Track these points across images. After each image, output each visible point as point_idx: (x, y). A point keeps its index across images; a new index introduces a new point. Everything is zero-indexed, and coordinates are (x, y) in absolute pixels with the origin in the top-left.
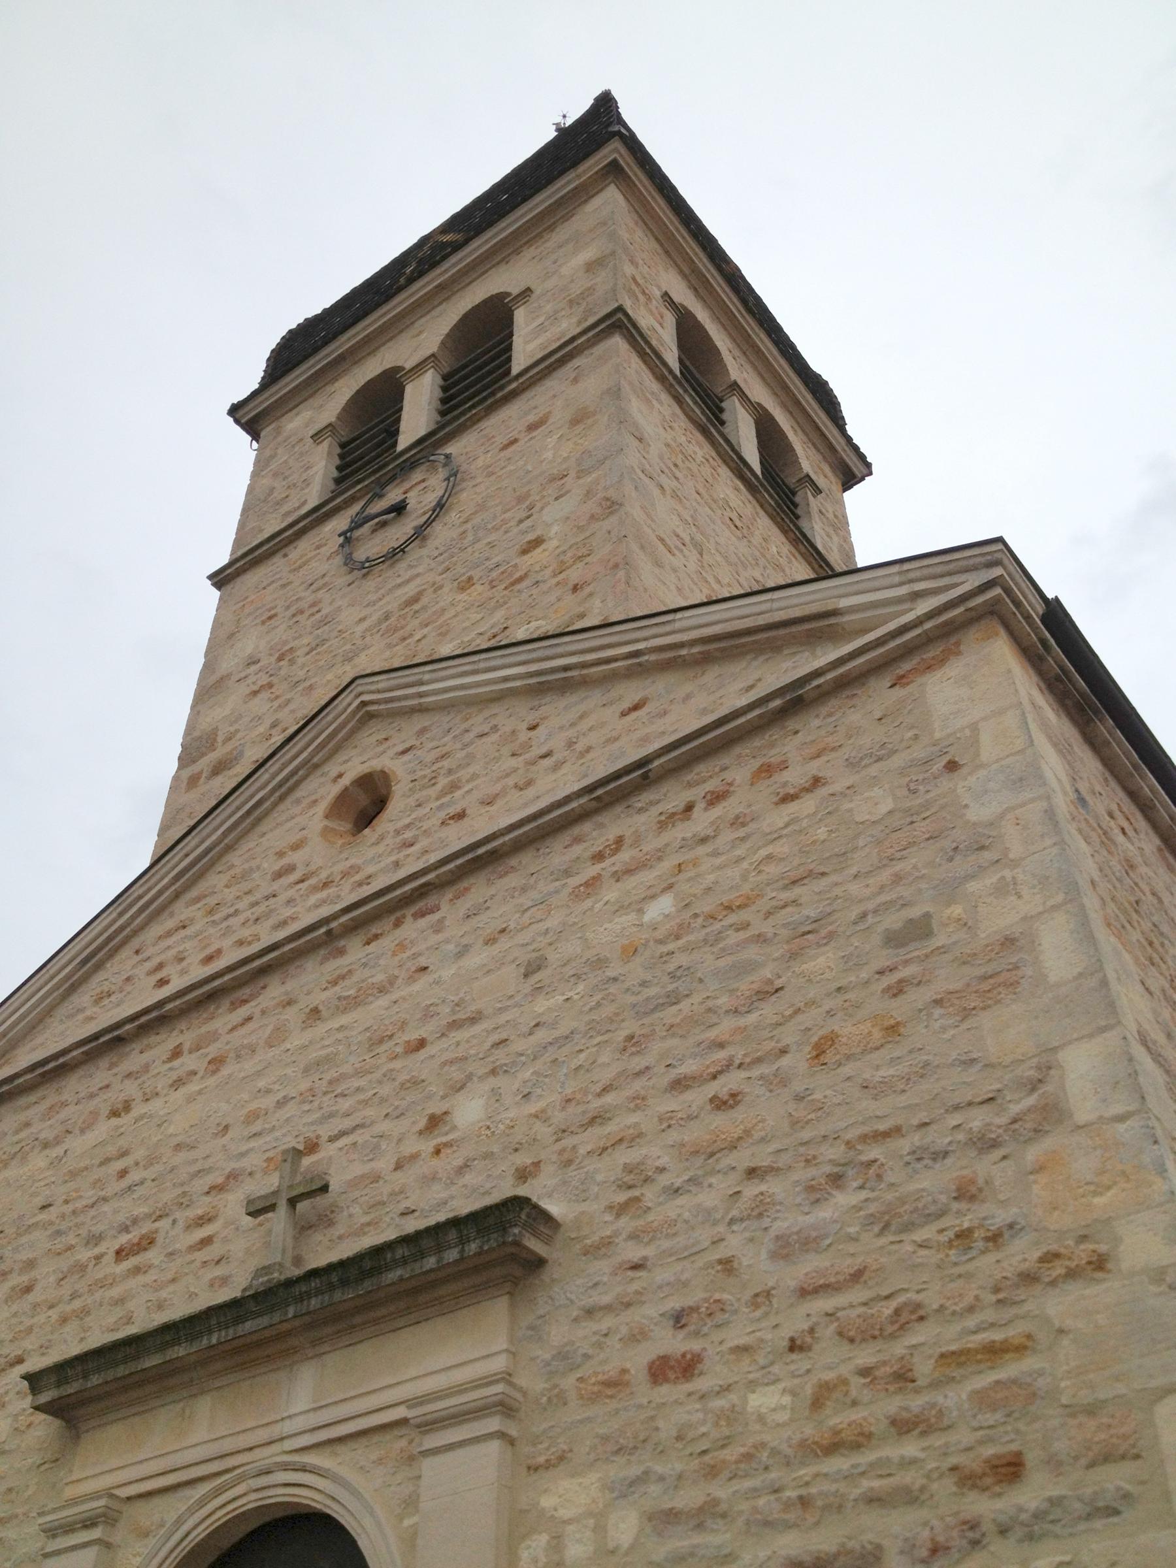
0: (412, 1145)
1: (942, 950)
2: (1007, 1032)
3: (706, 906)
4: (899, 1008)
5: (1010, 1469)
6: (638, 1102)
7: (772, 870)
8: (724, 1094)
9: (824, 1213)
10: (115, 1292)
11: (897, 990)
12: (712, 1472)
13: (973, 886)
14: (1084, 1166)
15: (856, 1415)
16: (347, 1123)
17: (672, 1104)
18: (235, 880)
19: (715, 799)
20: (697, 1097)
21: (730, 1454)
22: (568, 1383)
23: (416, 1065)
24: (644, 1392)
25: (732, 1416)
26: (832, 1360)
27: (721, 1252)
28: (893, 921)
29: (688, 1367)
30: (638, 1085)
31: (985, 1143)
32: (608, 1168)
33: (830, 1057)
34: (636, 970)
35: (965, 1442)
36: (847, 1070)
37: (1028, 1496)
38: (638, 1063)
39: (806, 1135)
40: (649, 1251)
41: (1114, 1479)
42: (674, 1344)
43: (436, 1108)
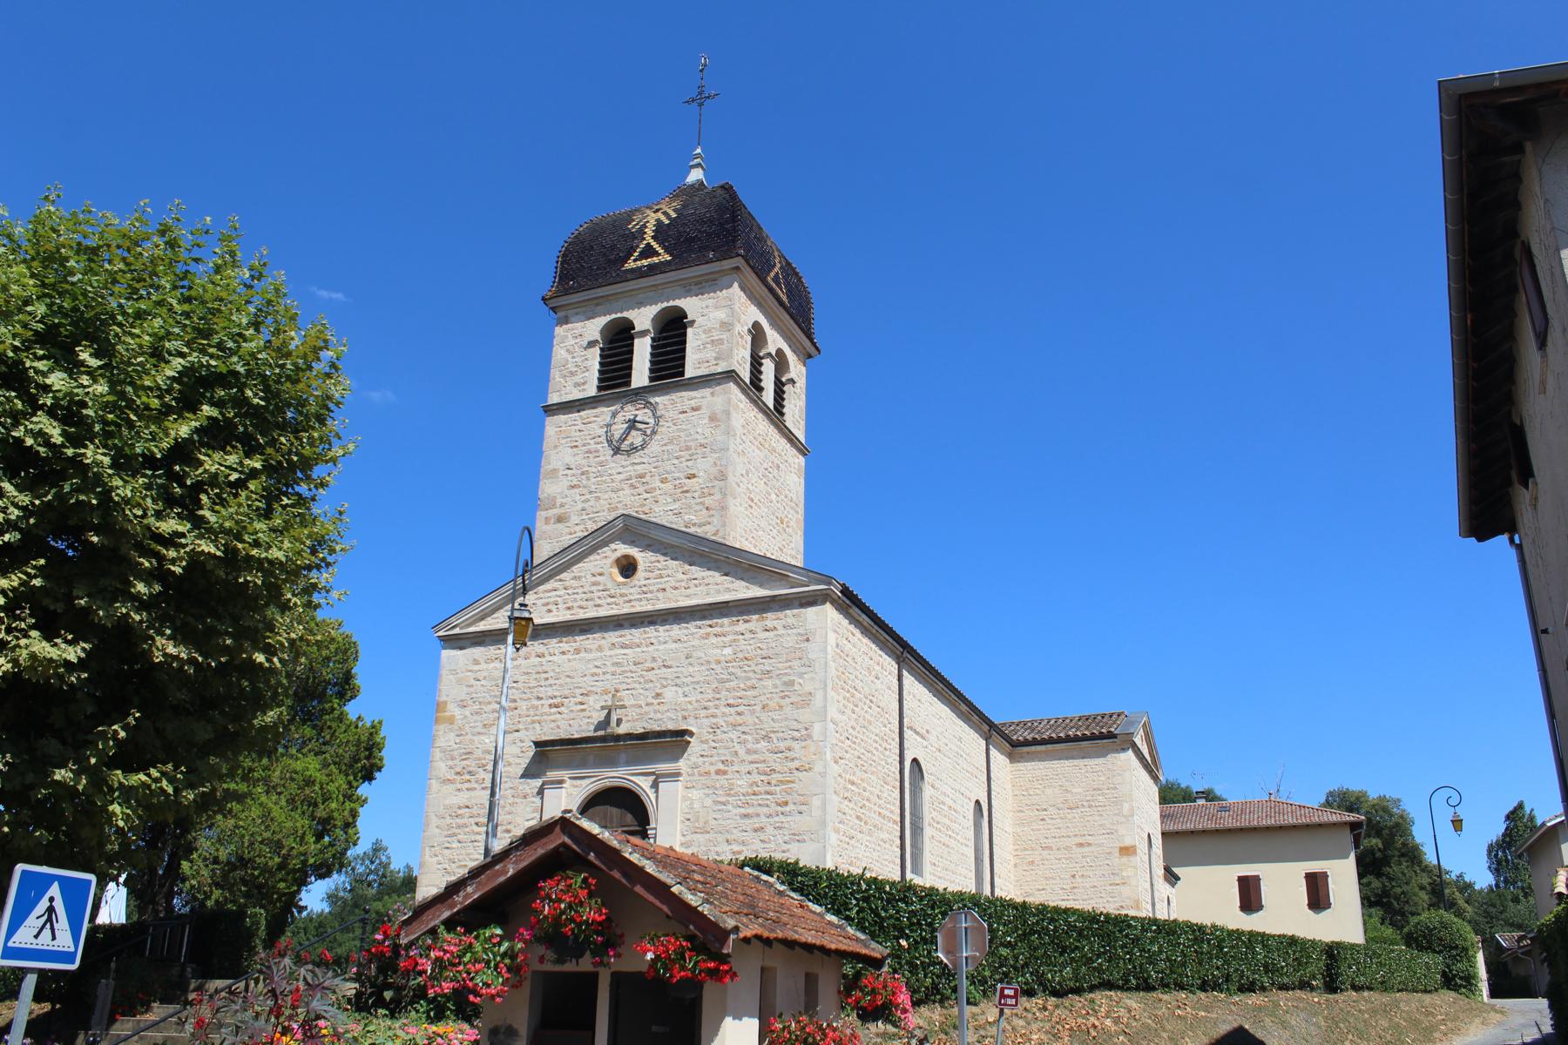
0: (650, 700)
2: (805, 715)
3: (741, 655)
4: (783, 702)
5: (786, 803)
6: (717, 707)
14: (812, 749)
18: (575, 578)
24: (714, 777)
26: (758, 778)
28: (786, 679)
29: (725, 773)
31: (794, 739)
34: (718, 668)
35: (780, 798)
37: (787, 809)
42: (721, 767)
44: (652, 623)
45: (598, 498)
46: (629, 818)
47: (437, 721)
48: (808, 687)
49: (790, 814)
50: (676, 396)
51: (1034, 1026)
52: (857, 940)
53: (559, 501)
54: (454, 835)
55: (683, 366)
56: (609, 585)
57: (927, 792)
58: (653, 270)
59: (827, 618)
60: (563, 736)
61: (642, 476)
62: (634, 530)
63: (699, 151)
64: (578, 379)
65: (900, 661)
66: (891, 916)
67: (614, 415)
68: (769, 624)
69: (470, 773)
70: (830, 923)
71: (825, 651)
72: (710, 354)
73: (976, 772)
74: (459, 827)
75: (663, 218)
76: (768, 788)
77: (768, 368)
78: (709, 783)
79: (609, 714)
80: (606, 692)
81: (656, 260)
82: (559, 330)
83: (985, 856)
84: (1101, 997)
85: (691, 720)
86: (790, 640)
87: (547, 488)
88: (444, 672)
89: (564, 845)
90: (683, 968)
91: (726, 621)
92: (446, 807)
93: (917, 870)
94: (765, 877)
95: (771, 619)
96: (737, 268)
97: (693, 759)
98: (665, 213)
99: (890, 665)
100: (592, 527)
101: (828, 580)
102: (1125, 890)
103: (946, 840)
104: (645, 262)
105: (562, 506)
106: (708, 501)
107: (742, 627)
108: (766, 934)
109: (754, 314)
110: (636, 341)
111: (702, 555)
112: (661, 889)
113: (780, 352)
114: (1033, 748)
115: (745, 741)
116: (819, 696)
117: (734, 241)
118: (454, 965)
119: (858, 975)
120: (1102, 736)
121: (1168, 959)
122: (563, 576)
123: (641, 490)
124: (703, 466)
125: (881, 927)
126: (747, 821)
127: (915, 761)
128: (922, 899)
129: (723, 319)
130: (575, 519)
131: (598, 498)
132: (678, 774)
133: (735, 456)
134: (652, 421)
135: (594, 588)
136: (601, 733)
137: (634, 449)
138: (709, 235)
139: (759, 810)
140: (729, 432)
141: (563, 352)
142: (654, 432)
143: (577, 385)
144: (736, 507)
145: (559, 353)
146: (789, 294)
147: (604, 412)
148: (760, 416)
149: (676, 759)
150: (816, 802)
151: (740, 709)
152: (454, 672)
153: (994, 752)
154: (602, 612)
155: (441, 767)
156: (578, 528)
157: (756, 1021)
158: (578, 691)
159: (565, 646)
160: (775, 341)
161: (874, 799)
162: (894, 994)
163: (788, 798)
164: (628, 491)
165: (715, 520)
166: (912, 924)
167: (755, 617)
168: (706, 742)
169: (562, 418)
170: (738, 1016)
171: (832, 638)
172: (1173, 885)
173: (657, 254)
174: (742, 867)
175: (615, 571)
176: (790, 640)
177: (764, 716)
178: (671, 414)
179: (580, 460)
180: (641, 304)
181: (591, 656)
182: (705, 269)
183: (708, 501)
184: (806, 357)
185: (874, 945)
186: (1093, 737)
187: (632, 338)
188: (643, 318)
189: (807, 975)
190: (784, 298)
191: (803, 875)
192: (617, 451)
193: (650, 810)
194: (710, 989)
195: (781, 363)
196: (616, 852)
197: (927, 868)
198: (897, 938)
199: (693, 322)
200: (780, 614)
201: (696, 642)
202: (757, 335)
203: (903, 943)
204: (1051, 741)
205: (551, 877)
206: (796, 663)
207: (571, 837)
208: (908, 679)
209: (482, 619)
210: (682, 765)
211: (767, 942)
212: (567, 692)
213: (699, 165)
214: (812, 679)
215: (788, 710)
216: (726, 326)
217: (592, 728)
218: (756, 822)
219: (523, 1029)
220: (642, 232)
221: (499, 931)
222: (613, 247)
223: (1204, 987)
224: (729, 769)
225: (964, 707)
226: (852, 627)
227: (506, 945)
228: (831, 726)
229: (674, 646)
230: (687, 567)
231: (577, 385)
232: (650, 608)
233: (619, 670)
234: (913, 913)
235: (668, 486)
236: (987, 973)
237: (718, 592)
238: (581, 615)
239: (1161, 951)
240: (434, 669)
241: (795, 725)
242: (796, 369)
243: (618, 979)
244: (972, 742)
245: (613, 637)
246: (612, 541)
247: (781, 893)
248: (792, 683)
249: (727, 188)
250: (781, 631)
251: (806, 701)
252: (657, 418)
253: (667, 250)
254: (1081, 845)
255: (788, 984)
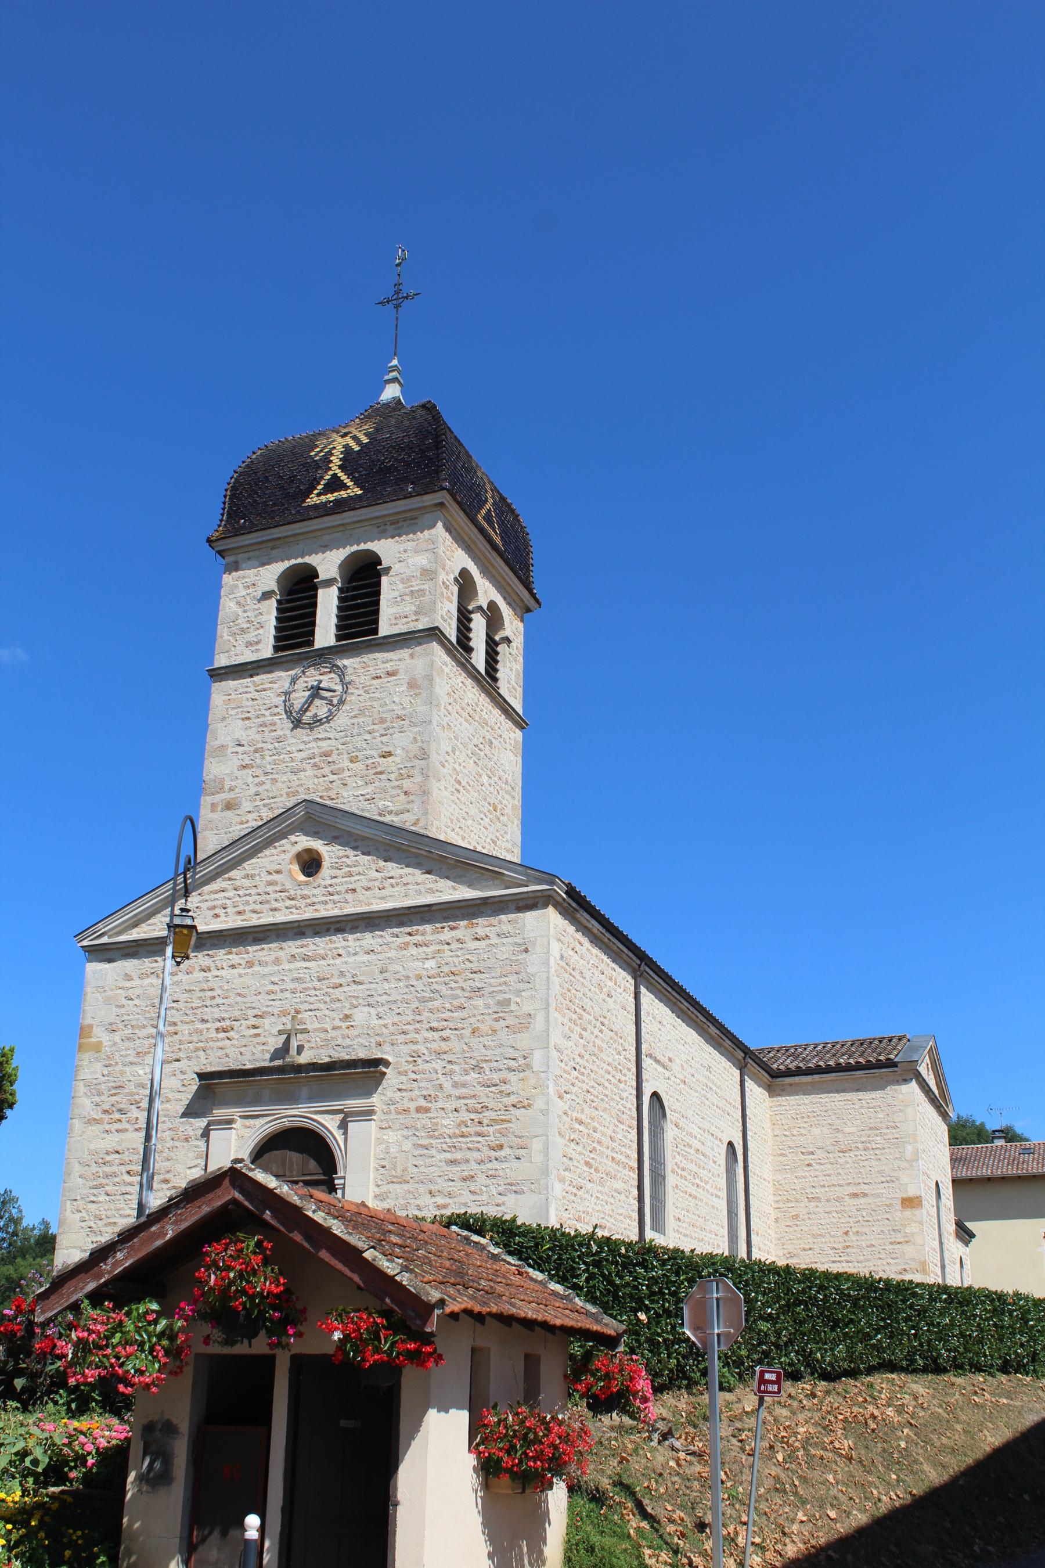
0: (338, 1023)
1: (512, 1011)
2: (523, 1040)
3: (446, 969)
5: (501, 1147)
7: (469, 965)
8: (444, 1036)
9: (467, 1078)
10: (219, 1044)
11: (497, 1020)
12: (432, 1137)
13: (523, 993)
14: (532, 1081)
15: (468, 1129)
16: (312, 1007)
17: (430, 1035)
18: (247, 876)
19: (452, 928)
20: (436, 1035)
21: (436, 1133)
22: (392, 1108)
23: (337, 993)
25: (436, 1124)
26: (465, 1116)
27: (438, 1082)
29: (427, 1110)
30: (418, 1025)
32: (405, 1049)
33: (476, 1034)
36: (481, 1039)
37: (502, 1153)
38: (418, 1018)
39: (466, 1055)
40: (418, 1077)
41: (521, 1152)
42: (423, 1103)
43: (347, 1012)
44: (340, 930)
45: (275, 780)
46: (312, 1164)
47: (81, 1048)
48: (527, 1008)
49: (505, 1159)
50: (368, 658)
51: (801, 1417)
52: (587, 1313)
53: (228, 783)
54: (102, 1186)
55: (376, 621)
56: (288, 885)
57: (670, 1133)
58: (340, 506)
59: (550, 925)
60: (234, 1066)
61: (327, 754)
62: (318, 818)
63: (395, 362)
64: (251, 636)
65: (637, 976)
66: (628, 1284)
67: (294, 681)
68: (480, 931)
69: (120, 1110)
70: (554, 1293)
71: (547, 963)
72: (409, 608)
73: (728, 1108)
74: (107, 1176)
75: (352, 444)
76: (479, 1129)
77: (479, 625)
78: (409, 1122)
79: (287, 1041)
80: (284, 1013)
81: (343, 494)
82: (227, 579)
83: (739, 1209)
84: (881, 1381)
85: (387, 1047)
86: (505, 951)
87: (214, 769)
88: (89, 989)
89: (234, 1201)
90: (378, 1350)
91: (428, 928)
92: (91, 1153)
93: (658, 1226)
94: (475, 1238)
95: (483, 925)
96: (441, 504)
97: (389, 1094)
98: (355, 438)
99: (624, 980)
100: (267, 815)
101: (550, 878)
102: (909, 1250)
103: (693, 1190)
104: (331, 497)
105: (231, 789)
106: (407, 784)
107: (447, 935)
108: (477, 1308)
109: (461, 560)
110: (320, 592)
111: (399, 849)
112: (351, 1255)
113: (492, 605)
114: (797, 1079)
115: (452, 1072)
116: (540, 1017)
117: (437, 472)
118: (101, 1348)
119: (588, 1356)
120: (879, 1065)
121: (962, 1335)
122: (233, 873)
123: (327, 770)
124: (401, 742)
125: (616, 1297)
126: (454, 1168)
127: (655, 1095)
128: (664, 1263)
129: (425, 565)
130: (247, 806)
131: (275, 780)
132: (372, 1112)
133: (438, 730)
134: (339, 688)
135: (270, 889)
136: (278, 1063)
137: (317, 722)
138: (407, 464)
139: (469, 1155)
140: (431, 701)
141: (232, 604)
142: (342, 702)
143: (249, 644)
144: (440, 791)
145: (228, 606)
146: (504, 534)
147: (281, 678)
148: (469, 682)
149: (369, 1093)
150: (536, 1145)
151: (447, 1033)
152: (101, 989)
153: (749, 1084)
154: (280, 918)
155: (85, 1105)
156: (250, 817)
157: (465, 1414)
158: (251, 1013)
159: (235, 958)
160: (486, 592)
161: (606, 1141)
162: (632, 1379)
163: (503, 1140)
164: (310, 772)
165: (415, 807)
166: (653, 1293)
167: (463, 923)
168: (405, 1073)
169: (231, 684)
170: (444, 1408)
171: (555, 948)
172: (967, 1243)
173: (345, 487)
174: (448, 1226)
175: (296, 868)
176: (505, 951)
177: (474, 1042)
178: (363, 679)
179: (253, 735)
180: (325, 548)
181: (266, 970)
182: (402, 505)
183: (407, 784)
184: (523, 611)
185: (607, 1319)
186: (869, 1066)
187: (315, 588)
188: (328, 564)
189: (527, 1357)
190: (498, 541)
191: (522, 1235)
192: (297, 724)
193: (338, 1154)
194: (410, 1376)
195: (494, 619)
196: (297, 1210)
197: (670, 1223)
198: (635, 1311)
199: (389, 569)
200: (493, 920)
201: (392, 954)
202: (465, 584)
203: (642, 1316)
204: (818, 1070)
205: (218, 1241)
206: (512, 979)
207: (242, 1192)
208: (647, 998)
209: (136, 925)
210: (376, 1100)
211: (479, 1318)
212: (237, 1014)
213: (395, 380)
214: (532, 997)
215: (503, 1034)
216: (428, 574)
217: (268, 1056)
218: (466, 1170)
219: (184, 1426)
220: (327, 460)
221: (155, 1306)
222: (292, 479)
223: (1005, 1368)
224: (433, 1106)
225: (713, 1030)
226: (579, 936)
227: (163, 1323)
228: (555, 1054)
229: (366, 958)
230: (381, 863)
231: (249, 644)
232: (337, 912)
233: (300, 987)
234: (654, 1280)
235: (359, 767)
236: (744, 1353)
237: (419, 893)
238: (255, 921)
239: (952, 1324)
240: (75, 990)
241: (512, 1053)
242: (512, 626)
243: (299, 1363)
244: (724, 1072)
245: (292, 947)
246: (292, 832)
247: (495, 1257)
248: (507, 1002)
249: (429, 408)
250: (494, 940)
251: (524, 1023)
252: (346, 685)
253: (357, 483)
254: (855, 1195)
255: (504, 1368)
